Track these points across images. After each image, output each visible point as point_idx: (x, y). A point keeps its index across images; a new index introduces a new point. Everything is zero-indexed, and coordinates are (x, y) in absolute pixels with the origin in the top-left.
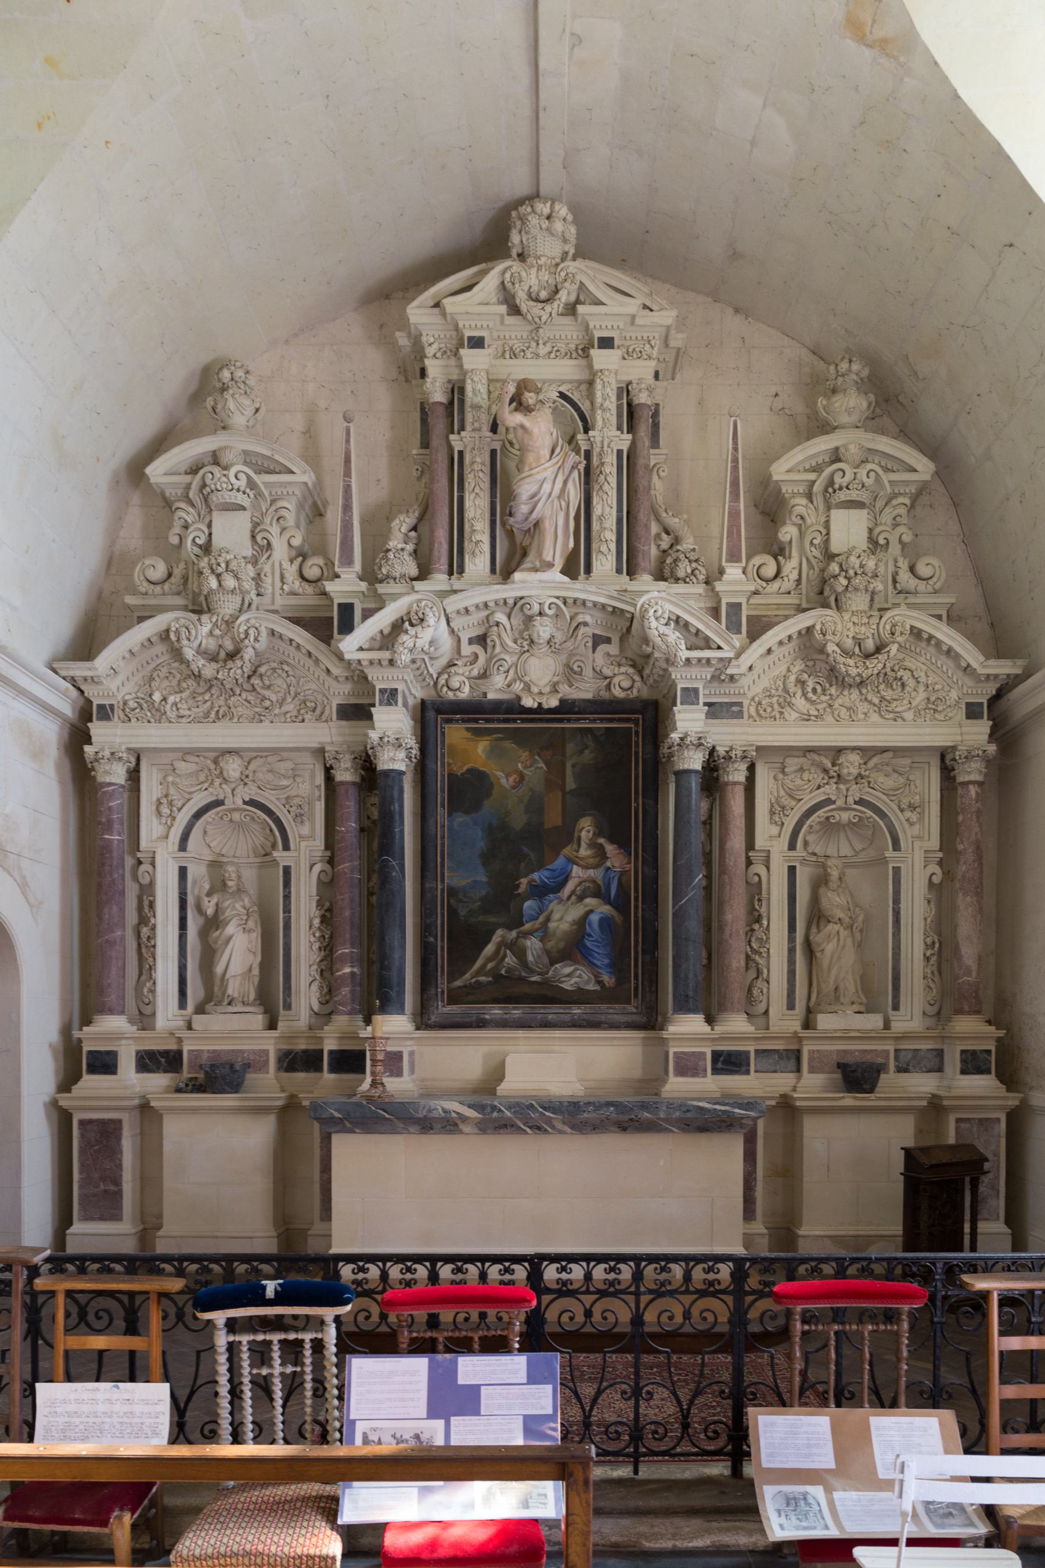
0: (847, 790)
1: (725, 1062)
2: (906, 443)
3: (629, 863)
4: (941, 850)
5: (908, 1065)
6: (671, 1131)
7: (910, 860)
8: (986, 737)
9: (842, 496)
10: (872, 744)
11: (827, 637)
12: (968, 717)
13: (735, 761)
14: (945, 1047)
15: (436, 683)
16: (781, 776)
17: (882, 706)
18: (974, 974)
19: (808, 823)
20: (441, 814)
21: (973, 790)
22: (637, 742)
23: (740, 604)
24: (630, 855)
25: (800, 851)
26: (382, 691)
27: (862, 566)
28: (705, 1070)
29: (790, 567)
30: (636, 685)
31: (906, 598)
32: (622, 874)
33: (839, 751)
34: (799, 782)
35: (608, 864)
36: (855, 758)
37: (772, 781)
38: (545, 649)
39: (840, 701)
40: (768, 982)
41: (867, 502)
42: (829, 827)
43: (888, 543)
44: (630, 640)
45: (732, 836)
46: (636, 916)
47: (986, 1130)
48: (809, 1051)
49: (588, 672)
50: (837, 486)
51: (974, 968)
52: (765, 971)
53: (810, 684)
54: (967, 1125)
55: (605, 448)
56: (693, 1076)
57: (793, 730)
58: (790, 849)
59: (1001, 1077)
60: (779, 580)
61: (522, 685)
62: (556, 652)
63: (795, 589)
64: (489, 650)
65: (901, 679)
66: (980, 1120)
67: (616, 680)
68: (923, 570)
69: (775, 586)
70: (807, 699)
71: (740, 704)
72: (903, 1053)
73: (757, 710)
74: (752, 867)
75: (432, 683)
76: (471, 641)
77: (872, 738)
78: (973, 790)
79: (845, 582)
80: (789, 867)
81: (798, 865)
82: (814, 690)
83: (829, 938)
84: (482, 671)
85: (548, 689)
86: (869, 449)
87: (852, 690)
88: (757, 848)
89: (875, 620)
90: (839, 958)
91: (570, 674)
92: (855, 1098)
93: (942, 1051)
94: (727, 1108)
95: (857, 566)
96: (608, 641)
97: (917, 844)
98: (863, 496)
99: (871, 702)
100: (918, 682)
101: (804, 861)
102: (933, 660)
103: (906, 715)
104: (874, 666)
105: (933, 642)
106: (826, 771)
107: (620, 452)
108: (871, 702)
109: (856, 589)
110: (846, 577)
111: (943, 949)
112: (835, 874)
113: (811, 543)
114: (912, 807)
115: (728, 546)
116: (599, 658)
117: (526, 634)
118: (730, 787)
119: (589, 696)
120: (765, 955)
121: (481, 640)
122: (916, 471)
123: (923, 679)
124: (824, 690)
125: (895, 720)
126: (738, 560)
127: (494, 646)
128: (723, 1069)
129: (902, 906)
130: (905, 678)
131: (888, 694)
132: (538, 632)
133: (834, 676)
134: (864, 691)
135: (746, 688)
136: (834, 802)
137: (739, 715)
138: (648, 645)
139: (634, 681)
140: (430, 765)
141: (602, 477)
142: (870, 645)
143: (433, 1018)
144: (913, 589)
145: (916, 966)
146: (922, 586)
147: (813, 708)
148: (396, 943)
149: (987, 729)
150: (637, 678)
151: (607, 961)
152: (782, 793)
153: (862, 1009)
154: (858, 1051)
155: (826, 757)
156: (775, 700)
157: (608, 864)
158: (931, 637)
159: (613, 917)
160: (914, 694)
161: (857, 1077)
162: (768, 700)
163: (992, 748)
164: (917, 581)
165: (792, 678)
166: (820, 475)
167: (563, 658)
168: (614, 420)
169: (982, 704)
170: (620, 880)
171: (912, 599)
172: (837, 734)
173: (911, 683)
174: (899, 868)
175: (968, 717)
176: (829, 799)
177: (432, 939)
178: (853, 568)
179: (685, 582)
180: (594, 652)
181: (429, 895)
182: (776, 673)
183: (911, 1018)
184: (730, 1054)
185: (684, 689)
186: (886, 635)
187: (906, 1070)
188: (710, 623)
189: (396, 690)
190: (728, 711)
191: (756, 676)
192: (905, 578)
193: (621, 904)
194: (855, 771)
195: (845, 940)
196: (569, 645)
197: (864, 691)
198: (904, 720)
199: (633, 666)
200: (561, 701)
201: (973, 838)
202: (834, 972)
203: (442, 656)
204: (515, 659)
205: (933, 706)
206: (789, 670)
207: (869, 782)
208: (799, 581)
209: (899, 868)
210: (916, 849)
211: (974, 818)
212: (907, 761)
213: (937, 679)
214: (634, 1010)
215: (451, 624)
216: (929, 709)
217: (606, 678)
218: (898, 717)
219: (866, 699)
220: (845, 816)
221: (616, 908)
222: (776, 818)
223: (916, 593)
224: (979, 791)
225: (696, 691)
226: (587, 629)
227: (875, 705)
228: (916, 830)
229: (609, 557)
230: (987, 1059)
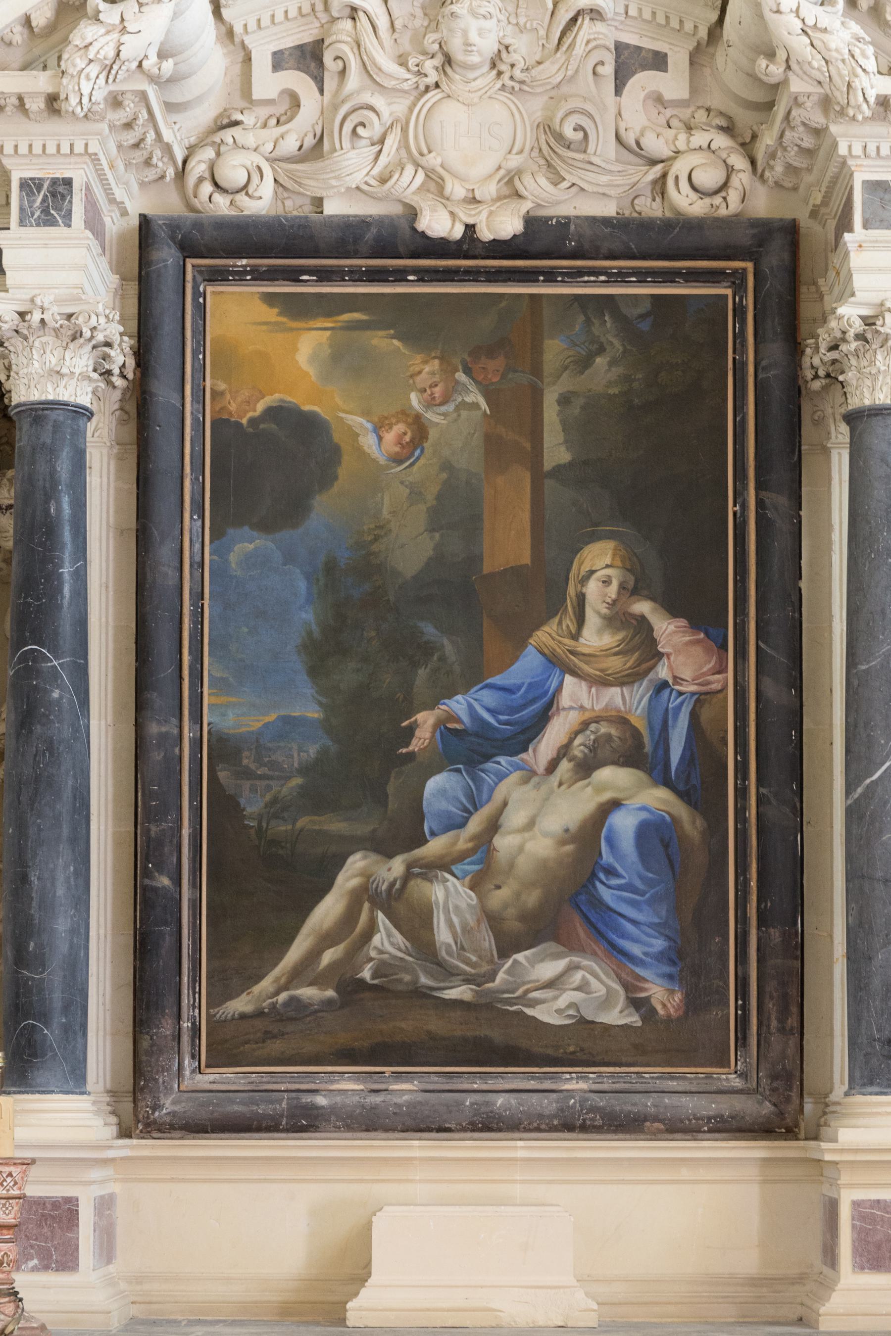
3: (721, 669)
15: (181, 174)
20: (193, 530)
22: (739, 337)
24: (724, 646)
26: (29, 186)
30: (735, 181)
32: (701, 699)
35: (663, 672)
38: (485, 79)
44: (720, 59)
46: (740, 812)
49: (604, 147)
61: (421, 176)
62: (517, 88)
64: (330, 84)
67: (680, 168)
75: (171, 173)
76: (279, 62)
84: (309, 141)
85: (491, 189)
91: (556, 145)
96: (659, 62)
116: (634, 110)
117: (431, 42)
119: (609, 209)
121: (310, 57)
127: (343, 72)
132: (465, 33)
138: (771, 55)
139: (730, 170)
140: (163, 392)
143: (169, 1105)
148: (60, 891)
150: (739, 162)
157: (663, 672)
167: (535, 107)
170: (694, 716)
177: (165, 881)
180: (618, 91)
181: (157, 756)
189: (68, 182)
193: (698, 782)
196: (552, 71)
199: (729, 130)
200: (530, 221)
203: (199, 99)
204: (400, 107)
214: (737, 1082)
215: (225, 13)
217: (653, 162)
221: (684, 795)
226: (599, 27)
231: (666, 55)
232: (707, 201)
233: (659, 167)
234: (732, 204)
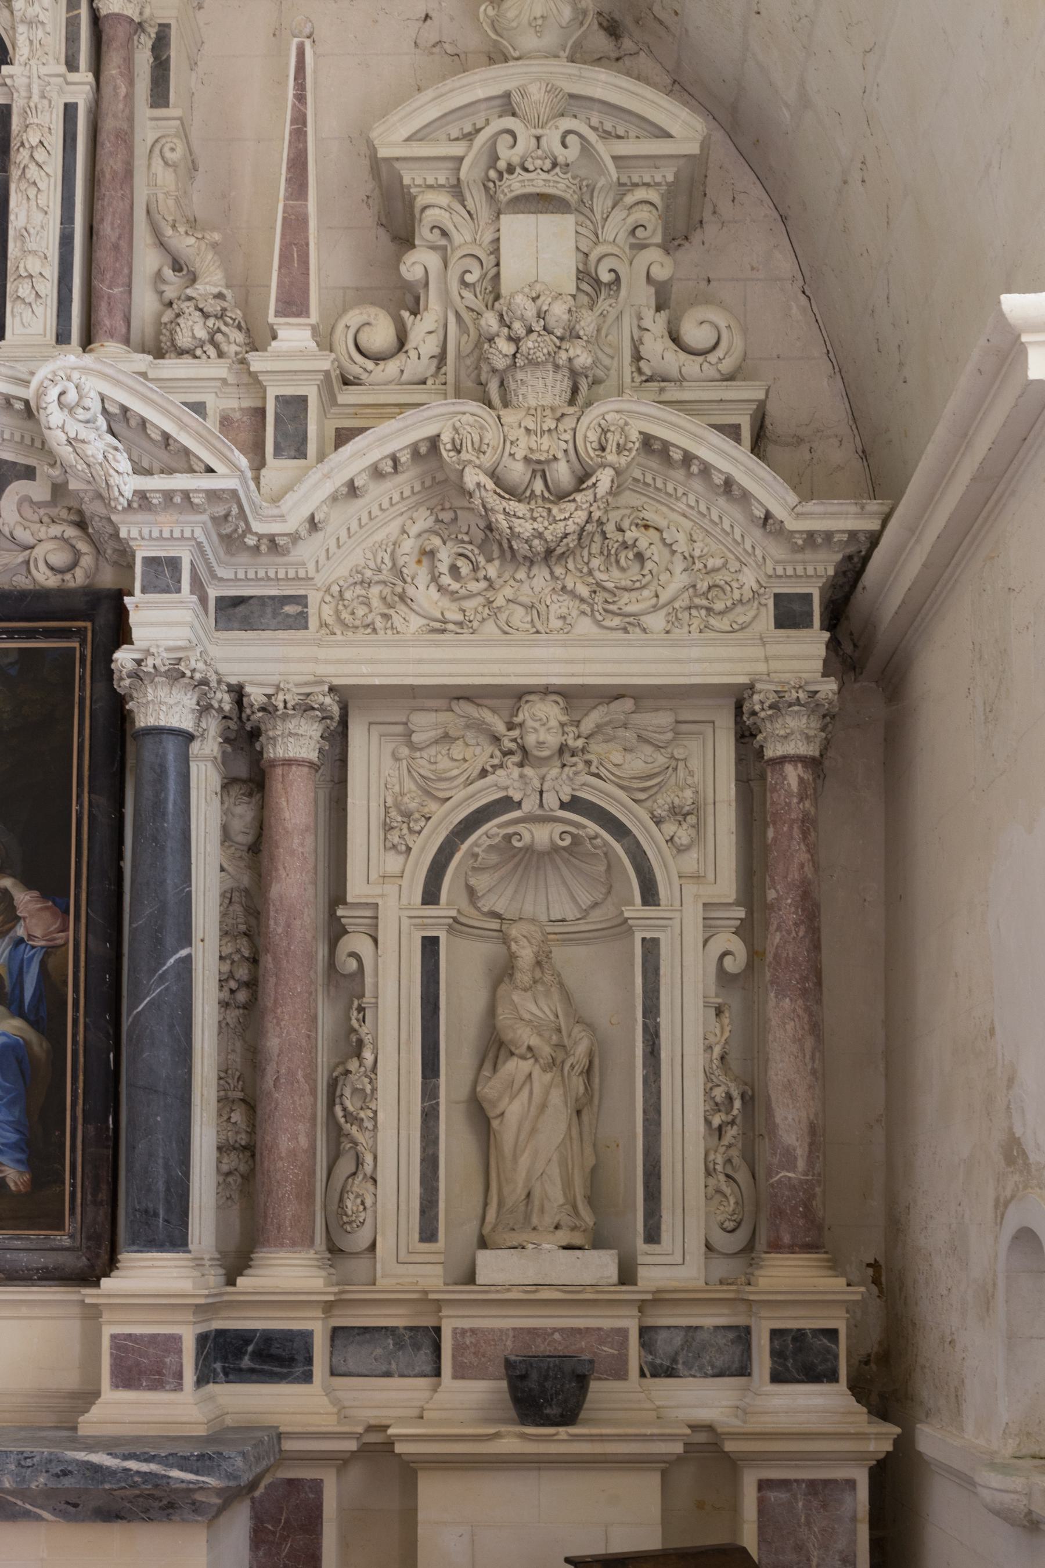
0: (543, 779)
1: (257, 1355)
2: (685, 104)
3: (64, 929)
4: (737, 903)
5: (674, 1361)
6: (39, 1518)
7: (677, 922)
8: (819, 665)
9: (516, 185)
10: (579, 681)
11: (464, 456)
12: (780, 624)
13: (285, 717)
14: (753, 1323)
16: (405, 751)
17: (602, 604)
18: (801, 1164)
19: (464, 847)
21: (793, 775)
22: (82, 678)
23: (303, 400)
24: (66, 912)
25: (443, 910)
27: (541, 315)
28: (179, 1375)
29: (423, 333)
31: (662, 390)
32: (49, 951)
33: (520, 695)
34: (444, 763)
35: (20, 931)
36: (550, 711)
37: (388, 762)
39: (508, 592)
40: (375, 1181)
41: (572, 198)
42: (521, 860)
43: (618, 279)
45: (282, 873)
47: (824, 1506)
48: (455, 1330)
50: (502, 165)
51: (801, 1152)
52: (369, 1159)
53: (445, 556)
54: (783, 1496)
55: (36, 98)
56: (152, 1388)
57: (413, 653)
58: (425, 902)
59: (858, 1389)
60: (402, 356)
63: (435, 375)
65: (634, 545)
66: (812, 1483)
67: (39, 552)
68: (695, 334)
69: (392, 367)
70: (440, 589)
71: (301, 600)
72: (663, 1335)
73: (337, 612)
74: (345, 939)
77: (578, 668)
78: (793, 775)
79: (508, 348)
80: (424, 939)
81: (443, 936)
82: (454, 570)
83: (512, 1089)
86: (572, 96)
87: (535, 570)
88: (349, 899)
89: (568, 423)
90: (533, 1131)
92: (523, 1436)
93: (748, 1330)
94: (153, 1467)
95: (530, 313)
97: (690, 889)
98: (558, 185)
99: (573, 594)
100: (674, 552)
101: (456, 925)
102: (703, 508)
103: (648, 621)
104: (571, 516)
105: (695, 469)
106: (496, 739)
107: (70, 110)
108: (573, 594)
109: (533, 363)
110: (510, 339)
111: (743, 1109)
112: (526, 954)
113: (464, 283)
114: (678, 814)
115: (280, 285)
118: (279, 771)
120: (369, 1125)
122: (670, 136)
123: (682, 547)
124: (475, 569)
125: (625, 630)
126: (302, 311)
128: (252, 1371)
129: (664, 1020)
130: (643, 544)
131: (612, 578)
133: (495, 543)
134: (559, 571)
135: (311, 567)
136: (519, 804)
137: (300, 622)
139: (77, 554)
141: (24, 153)
142: (562, 473)
144: (674, 373)
145: (690, 1149)
146: (692, 366)
147: (454, 606)
149: (820, 650)
150: (83, 546)
151: (13, 1137)
152: (409, 785)
153: (577, 1241)
154: (561, 1330)
155: (494, 711)
156: (375, 590)
157: (20, 931)
158: (688, 458)
159: (27, 1043)
160: (664, 577)
161: (546, 1389)
162: (359, 590)
163: (829, 687)
164: (682, 355)
165: (408, 545)
166: (470, 147)
168: (57, 44)
169: (808, 597)
170: (43, 964)
171: (673, 393)
172: (505, 661)
173: (656, 553)
174: (655, 942)
175: (780, 624)
176: (508, 799)
178: (522, 318)
179: (195, 357)
182: (379, 536)
183: (676, 1263)
184: (268, 1337)
185: (148, 561)
186: (589, 453)
187: (670, 1373)
188: (186, 419)
190: (275, 614)
191: (332, 543)
192: (658, 350)
193: (45, 1013)
194: (553, 740)
195: (547, 1093)
197: (559, 571)
198: (644, 630)
201: (795, 875)
202: (524, 1160)
205: (705, 601)
206: (404, 532)
207: (588, 763)
208: (441, 358)
209: (655, 942)
210: (688, 899)
211: (796, 833)
212: (664, 719)
213: (714, 547)
214: (66, 1242)
216: (697, 607)
218: (632, 623)
219: (564, 588)
220: (542, 835)
221: (34, 1024)
222: (394, 837)
223: (681, 380)
224: (808, 776)
225: (174, 563)
227: (582, 600)
228: (690, 862)
229: (39, 310)
230: (828, 1351)
231: (35, 468)
232: (59, 576)
233: (28, 552)
234: (78, 579)
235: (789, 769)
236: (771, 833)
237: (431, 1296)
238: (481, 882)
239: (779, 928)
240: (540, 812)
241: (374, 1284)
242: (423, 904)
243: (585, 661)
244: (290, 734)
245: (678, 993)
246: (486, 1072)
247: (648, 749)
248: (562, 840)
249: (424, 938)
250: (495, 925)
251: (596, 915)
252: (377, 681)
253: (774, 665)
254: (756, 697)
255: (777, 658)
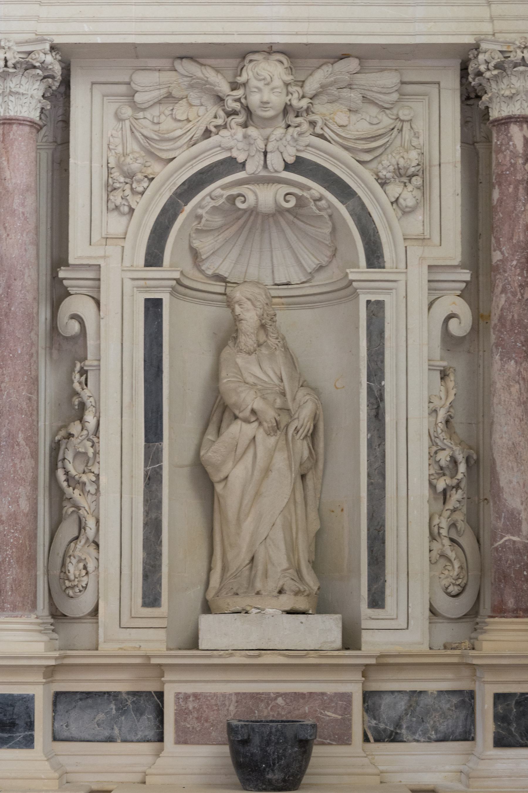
0: (267, 140)
4: (462, 266)
5: (398, 725)
7: (402, 284)
16: (127, 112)
19: (188, 208)
25: (167, 272)
33: (243, 54)
34: (167, 124)
36: (274, 70)
37: (111, 123)
40: (97, 545)
52: (91, 523)
72: (387, 700)
74: (67, 301)
81: (166, 298)
83: (236, 454)
88: (71, 261)
90: (257, 494)
93: (471, 694)
97: (415, 251)
101: (179, 287)
106: (220, 99)
112: (250, 317)
114: (404, 175)
120: (91, 488)
129: (389, 383)
136: (243, 165)
145: (414, 513)
152: (132, 146)
153: (301, 604)
155: (217, 71)
174: (380, 304)
183: (402, 626)
187: (394, 737)
194: (278, 100)
202: (248, 525)
207: (313, 124)
209: (380, 304)
210: (413, 260)
212: (389, 79)
220: (266, 197)
222: (117, 198)
228: (415, 224)
235: (514, 129)
236: (496, 194)
237: (154, 661)
238: (205, 245)
239: (504, 290)
240: (264, 173)
241: (97, 649)
242: (146, 266)
243: (309, 20)
244: (11, 93)
245: (403, 356)
246: (210, 436)
247: (373, 111)
248: (287, 201)
249: (147, 300)
250: (219, 288)
251: (321, 278)
252: (99, 40)
253: (499, 25)
254: (481, 57)
255: (502, 18)
